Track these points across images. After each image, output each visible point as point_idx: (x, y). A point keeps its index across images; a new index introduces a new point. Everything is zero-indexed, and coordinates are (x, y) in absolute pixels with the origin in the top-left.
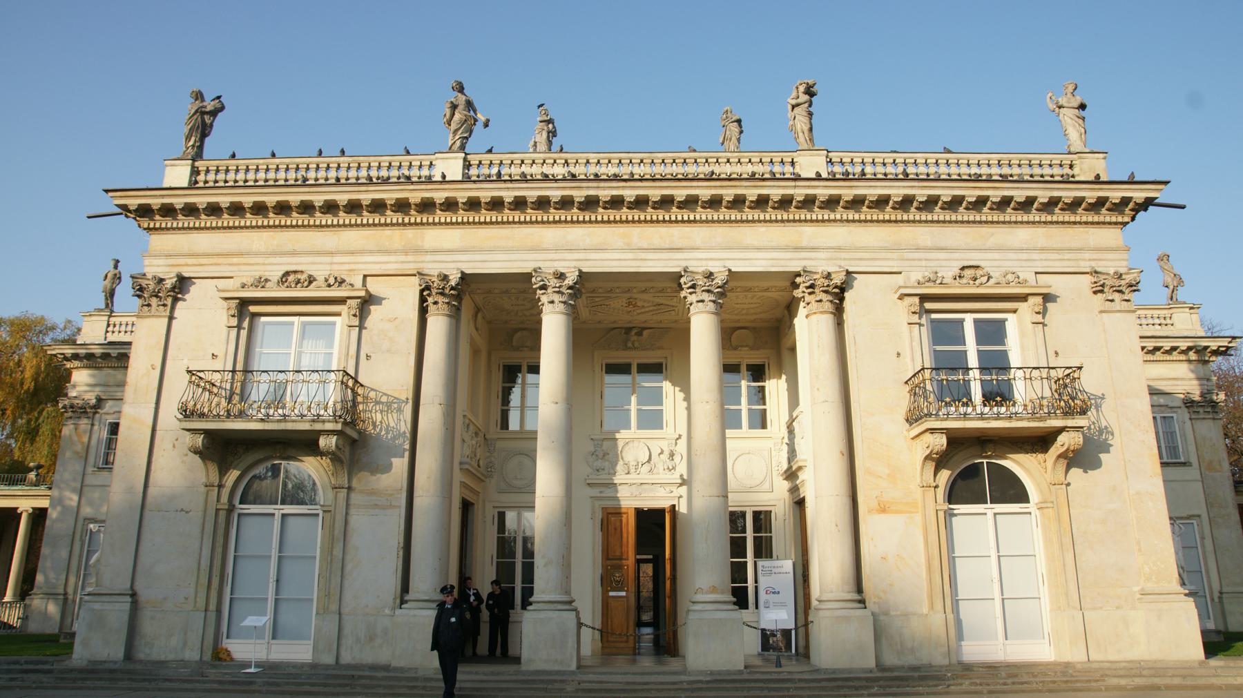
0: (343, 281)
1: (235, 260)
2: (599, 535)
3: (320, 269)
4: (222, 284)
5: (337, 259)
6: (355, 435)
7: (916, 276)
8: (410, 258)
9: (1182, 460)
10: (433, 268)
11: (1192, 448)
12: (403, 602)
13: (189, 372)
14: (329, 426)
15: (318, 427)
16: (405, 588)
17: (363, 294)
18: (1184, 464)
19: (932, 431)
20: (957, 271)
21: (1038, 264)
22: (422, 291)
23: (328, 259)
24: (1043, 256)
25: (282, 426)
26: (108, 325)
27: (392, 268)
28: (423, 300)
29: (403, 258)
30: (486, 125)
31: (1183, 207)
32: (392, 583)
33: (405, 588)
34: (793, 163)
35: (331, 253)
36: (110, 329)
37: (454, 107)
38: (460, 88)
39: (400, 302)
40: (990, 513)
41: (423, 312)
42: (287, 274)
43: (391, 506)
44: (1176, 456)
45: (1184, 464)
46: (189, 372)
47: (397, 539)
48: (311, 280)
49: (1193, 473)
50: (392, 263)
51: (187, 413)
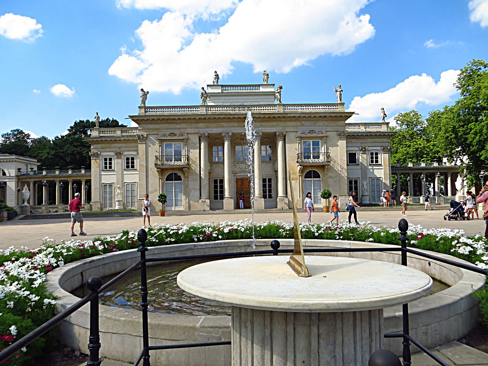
0: (182, 135)
2: (235, 184)
3: (177, 132)
4: (156, 136)
6: (188, 167)
8: (196, 130)
10: (202, 131)
12: (200, 198)
13: (155, 156)
16: (201, 196)
17: (187, 138)
19: (300, 165)
22: (199, 137)
23: (179, 130)
26: (99, 131)
28: (200, 138)
33: (201, 196)
35: (179, 129)
36: (100, 133)
37: (202, 94)
40: (312, 180)
41: (200, 141)
46: (155, 156)
48: (176, 135)
50: (192, 131)
51: (156, 164)
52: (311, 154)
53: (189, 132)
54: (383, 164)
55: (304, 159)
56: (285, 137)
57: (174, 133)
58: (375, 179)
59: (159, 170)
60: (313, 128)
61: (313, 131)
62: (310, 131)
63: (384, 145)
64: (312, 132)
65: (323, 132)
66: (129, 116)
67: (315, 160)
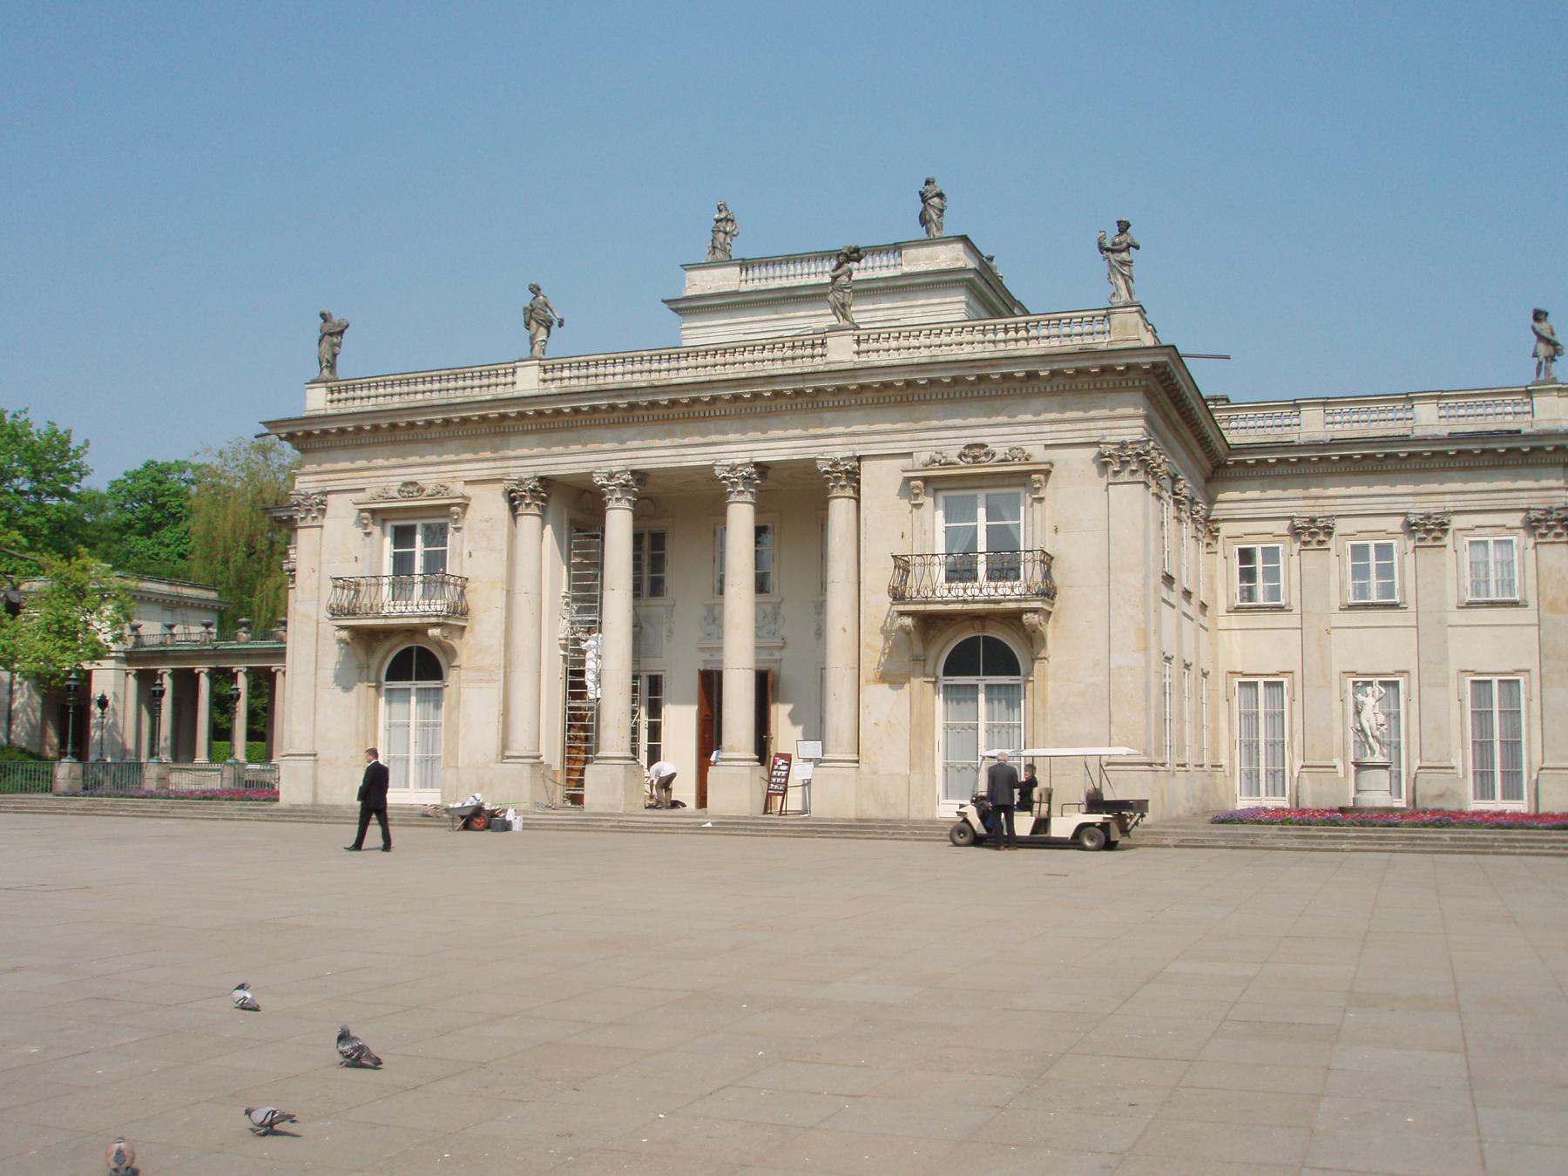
1: (366, 474)
5: (443, 468)
7: (925, 457)
8: (499, 464)
9: (1517, 598)
11: (1531, 582)
14: (433, 620)
15: (426, 620)
18: (1515, 604)
20: (960, 449)
21: (1049, 436)
24: (1054, 428)
25: (400, 621)
27: (485, 474)
28: (512, 500)
29: (492, 464)
30: (561, 325)
31: (1228, 357)
32: (493, 742)
33: (505, 745)
34: (823, 344)
38: (535, 290)
39: (489, 505)
42: (406, 484)
43: (493, 680)
44: (1511, 593)
45: (1515, 604)
47: (496, 708)
49: (1529, 615)
50: (484, 469)
52: (982, 558)
53: (473, 476)
54: (1532, 600)
55: (948, 580)
56: (854, 477)
57: (414, 483)
58: (1495, 679)
59: (344, 634)
60: (981, 435)
61: (983, 446)
62: (968, 447)
63: (1537, 501)
64: (976, 451)
65: (1028, 450)
66: (266, 423)
67: (965, 590)
